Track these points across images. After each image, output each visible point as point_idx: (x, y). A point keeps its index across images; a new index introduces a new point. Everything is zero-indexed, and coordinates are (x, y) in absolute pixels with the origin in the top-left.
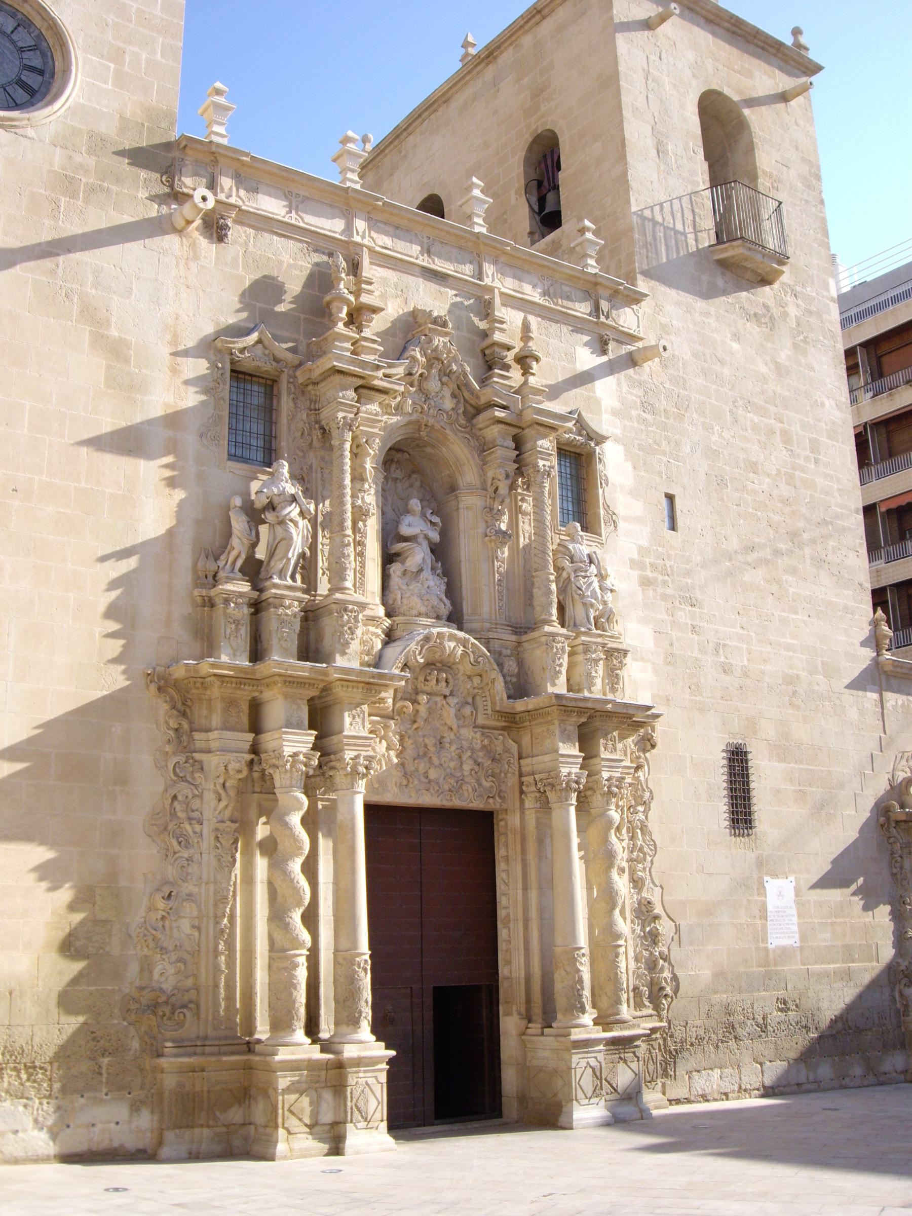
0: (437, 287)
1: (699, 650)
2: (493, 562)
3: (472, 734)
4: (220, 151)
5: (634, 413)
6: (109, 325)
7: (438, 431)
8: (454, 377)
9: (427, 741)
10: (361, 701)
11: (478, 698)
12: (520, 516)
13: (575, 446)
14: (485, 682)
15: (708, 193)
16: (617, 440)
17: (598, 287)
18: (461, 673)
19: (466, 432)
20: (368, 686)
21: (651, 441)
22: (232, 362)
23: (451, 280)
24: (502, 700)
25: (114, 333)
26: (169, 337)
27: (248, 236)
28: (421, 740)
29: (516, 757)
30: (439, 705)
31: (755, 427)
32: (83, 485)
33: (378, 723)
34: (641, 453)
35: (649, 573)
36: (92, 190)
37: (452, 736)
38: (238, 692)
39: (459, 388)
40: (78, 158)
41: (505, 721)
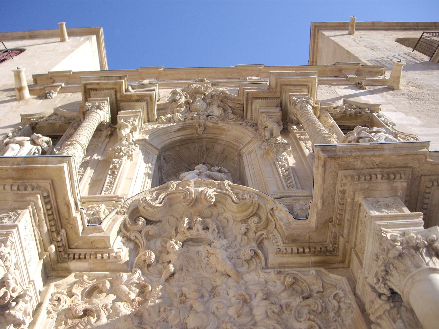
2: (275, 164)
3: (262, 274)
4: (53, 75)
7: (213, 128)
8: (215, 98)
9: (185, 290)
10: (16, 205)
11: (266, 242)
12: (301, 142)
14: (264, 218)
15: (415, 51)
17: (343, 71)
18: (231, 221)
20: (20, 182)
23: (220, 84)
24: (289, 223)
28: (176, 290)
29: (348, 289)
30: (204, 254)
33: (105, 277)
37: (231, 282)
39: (221, 101)
41: (314, 254)
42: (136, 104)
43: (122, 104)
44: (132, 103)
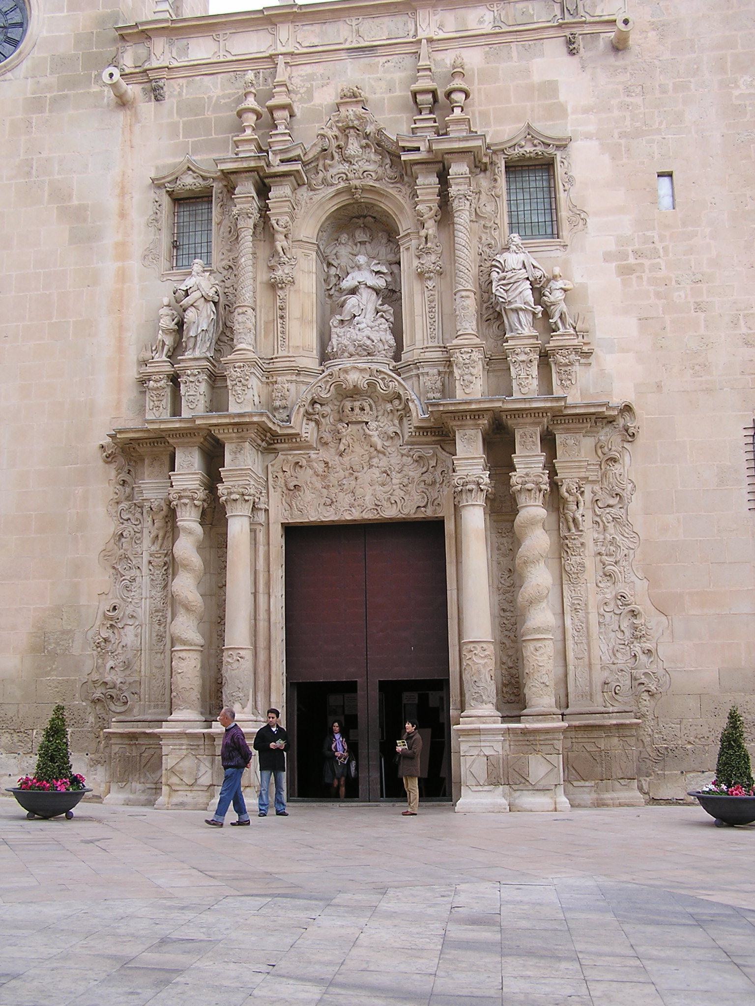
0: (367, 60)
1: (707, 327)
5: (614, 102)
6: (70, 196)
13: (530, 158)
16: (588, 137)
19: (396, 183)
21: (638, 124)
22: (170, 194)
25: (75, 202)
26: (117, 191)
27: (181, 87)
32: (54, 320)
34: (623, 141)
35: (632, 260)
36: (54, 100)
38: (155, 449)
40: (43, 80)
42: (282, 179)
43: (267, 181)
44: (276, 179)
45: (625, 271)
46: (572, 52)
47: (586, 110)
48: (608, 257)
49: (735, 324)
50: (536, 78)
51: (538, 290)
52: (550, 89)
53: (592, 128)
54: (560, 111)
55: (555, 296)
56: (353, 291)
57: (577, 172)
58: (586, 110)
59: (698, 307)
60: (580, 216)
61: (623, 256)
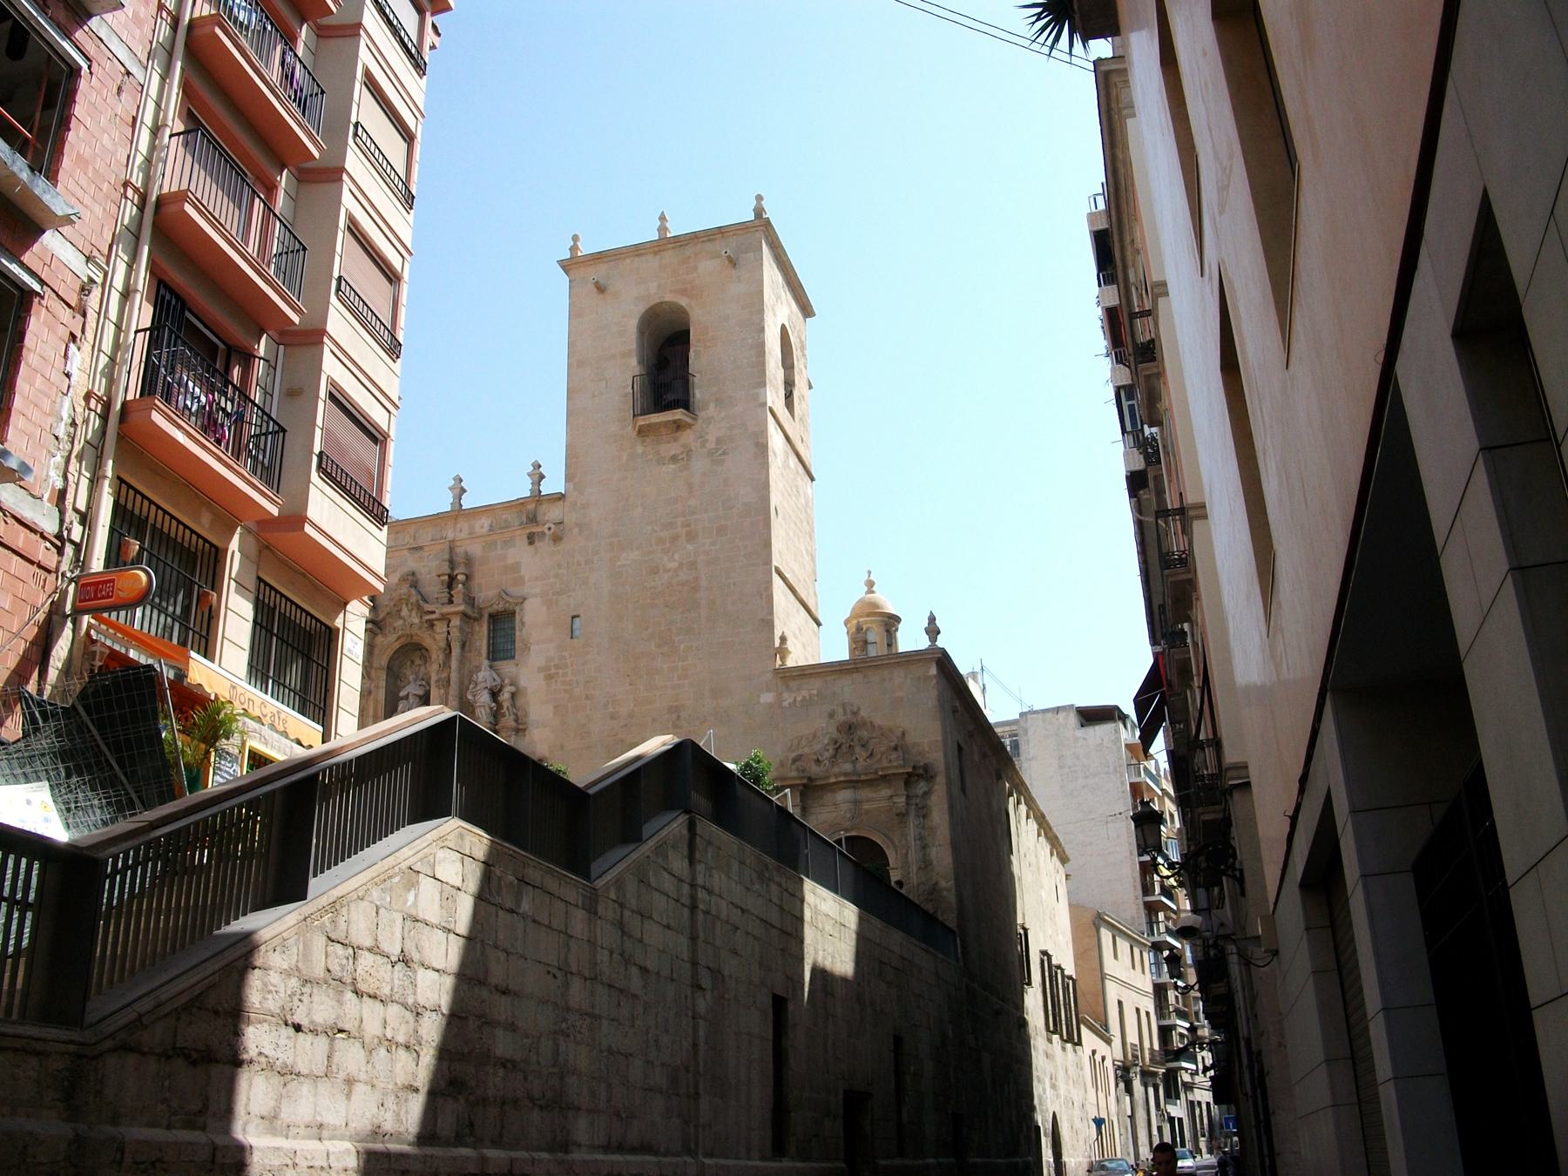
31: (660, 541)
45: (549, 677)
46: (531, 543)
47: (536, 579)
48: (540, 670)
49: (606, 706)
50: (510, 561)
51: (495, 694)
52: (516, 567)
53: (538, 590)
54: (520, 581)
55: (505, 696)
56: (406, 697)
57: (527, 619)
58: (536, 579)
59: (587, 697)
60: (527, 648)
61: (547, 668)
